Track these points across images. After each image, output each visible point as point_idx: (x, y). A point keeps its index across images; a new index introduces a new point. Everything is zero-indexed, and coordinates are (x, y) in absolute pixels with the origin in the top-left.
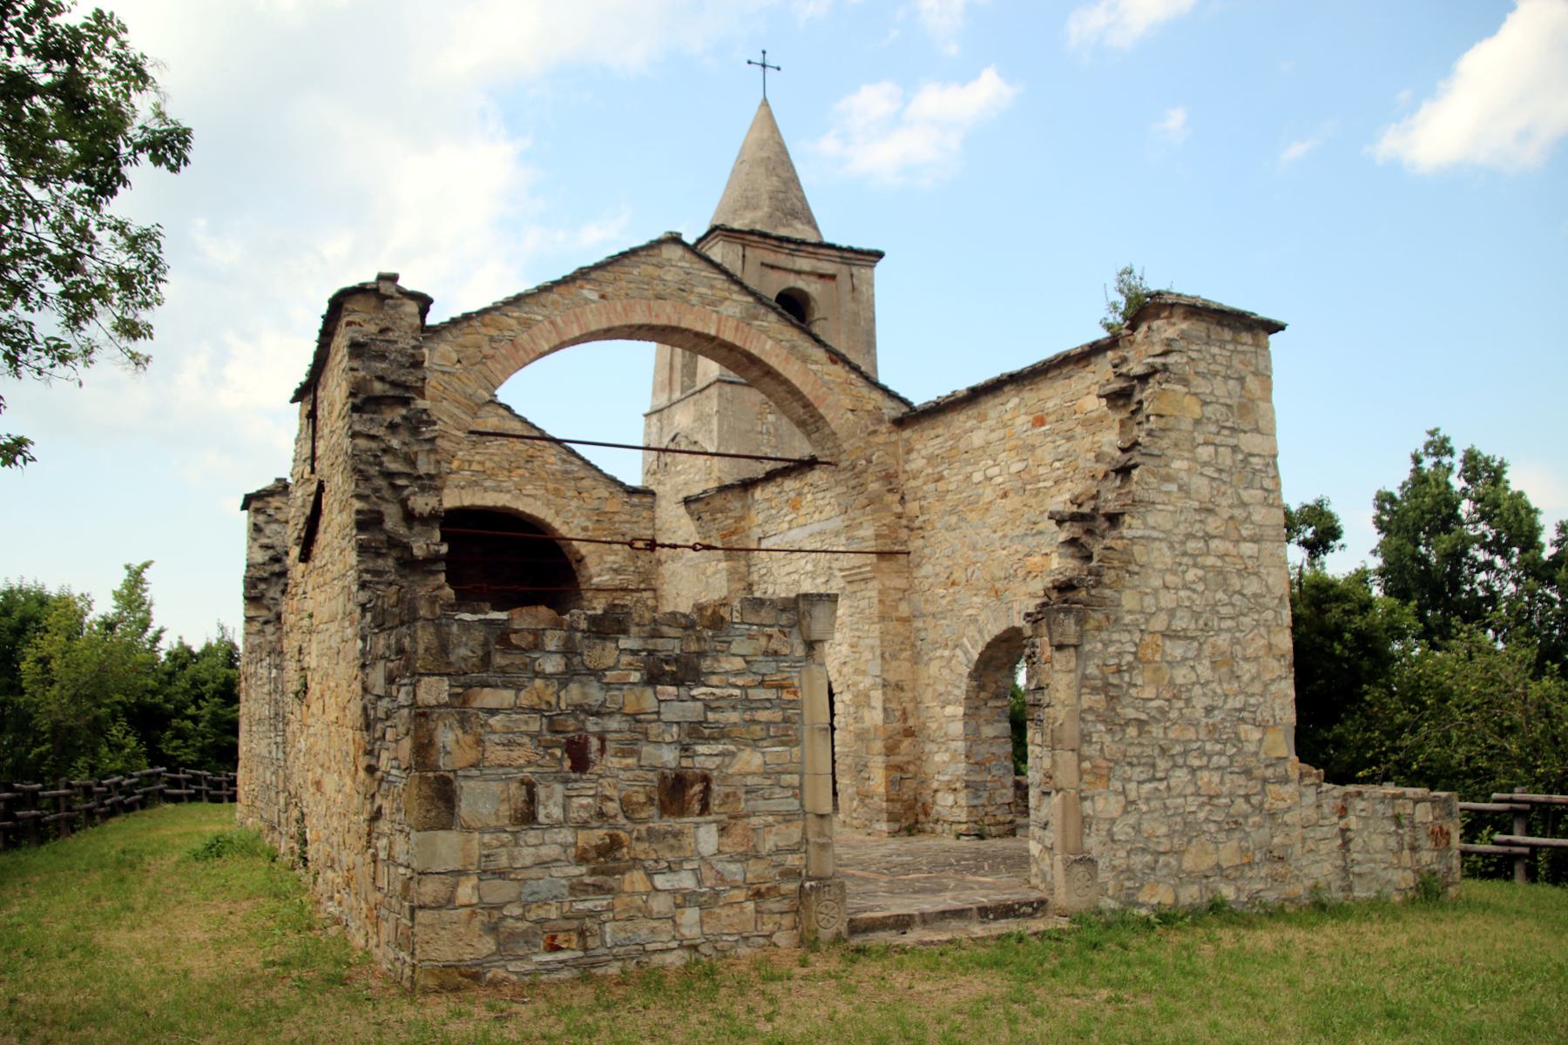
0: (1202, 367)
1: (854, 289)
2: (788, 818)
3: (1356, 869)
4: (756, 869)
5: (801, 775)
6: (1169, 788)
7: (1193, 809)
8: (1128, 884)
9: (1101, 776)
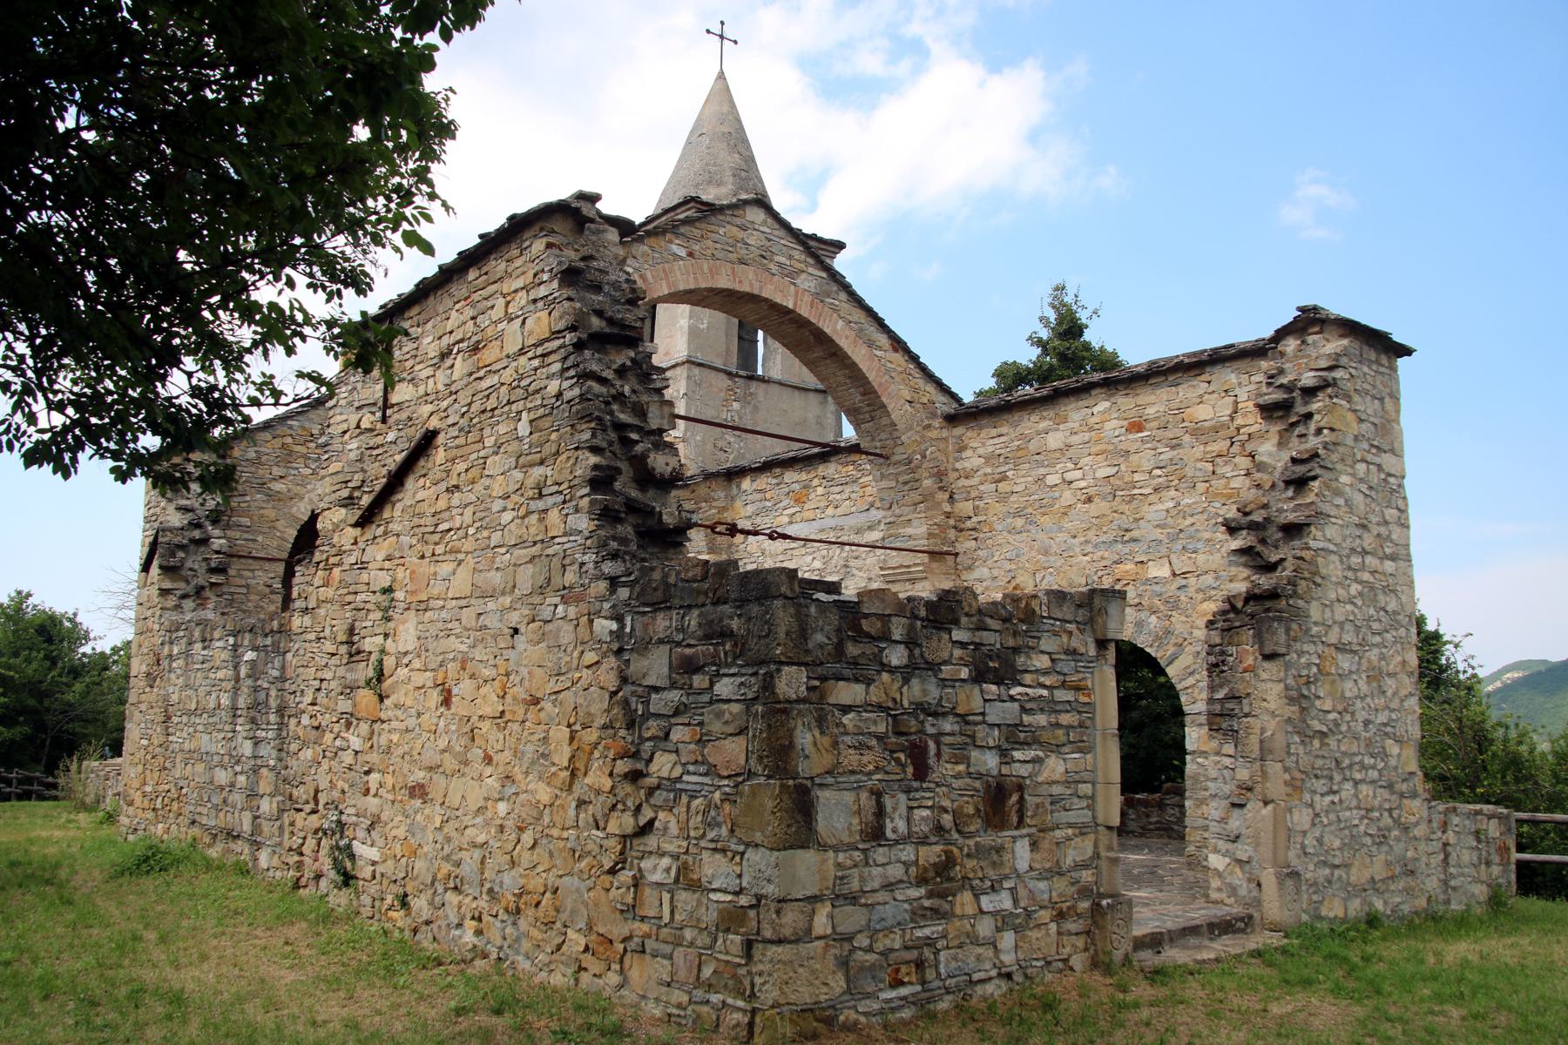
4: (1061, 884)
5: (1094, 784)
6: (1341, 801)
8: (1315, 898)
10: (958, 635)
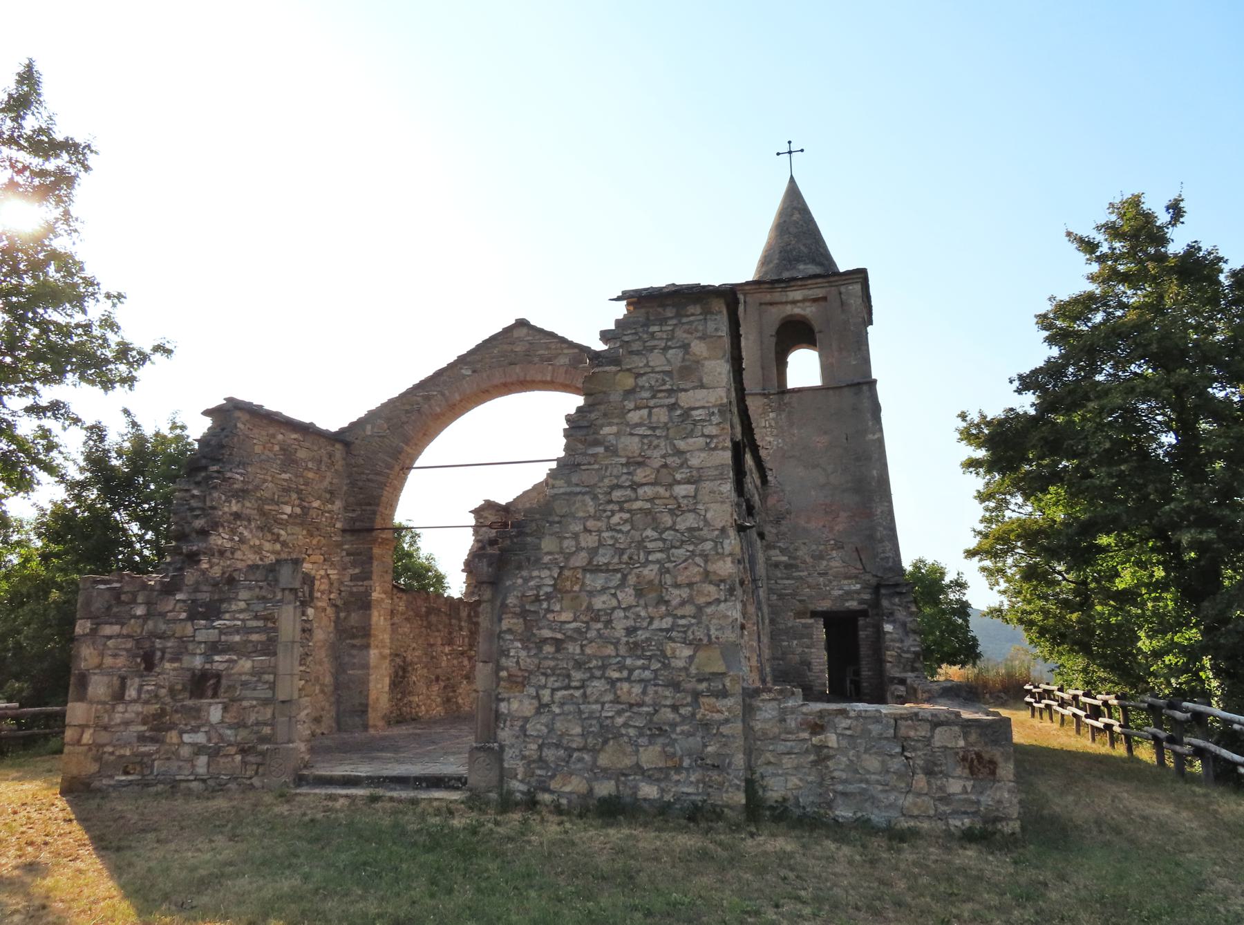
0: (636, 346)
1: (842, 303)
2: (266, 702)
3: (840, 788)
4: (243, 733)
5: (275, 675)
6: (584, 695)
7: (610, 714)
8: (539, 772)
9: (519, 682)
10: (178, 597)
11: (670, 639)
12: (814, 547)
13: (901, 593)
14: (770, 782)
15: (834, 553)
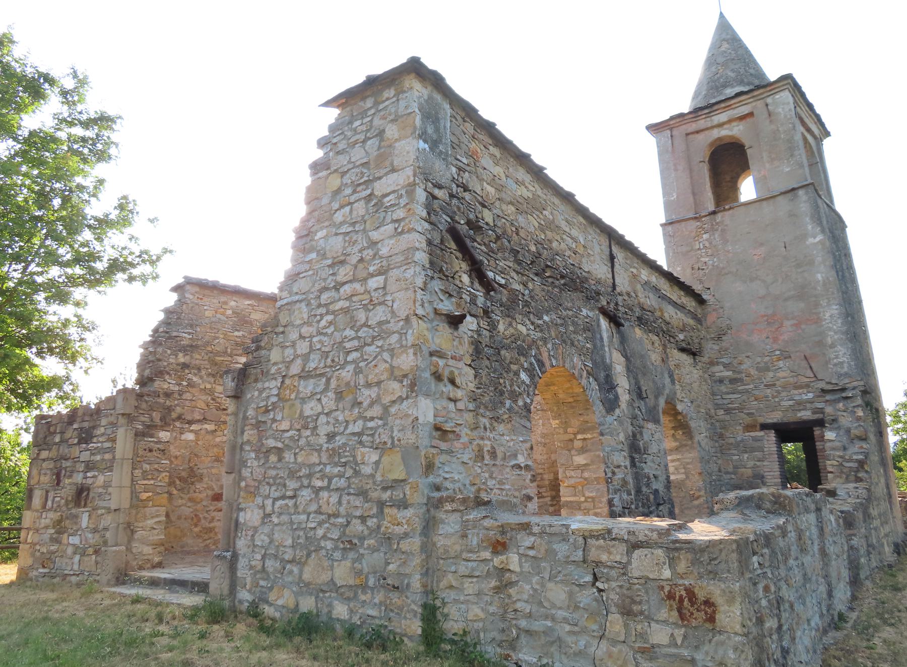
3: (523, 623)
6: (296, 506)
8: (262, 583)
11: (361, 443)
12: (759, 359)
13: (847, 398)
14: (452, 610)
15: (781, 364)
